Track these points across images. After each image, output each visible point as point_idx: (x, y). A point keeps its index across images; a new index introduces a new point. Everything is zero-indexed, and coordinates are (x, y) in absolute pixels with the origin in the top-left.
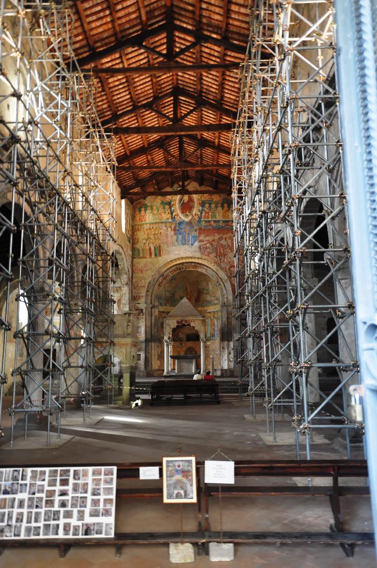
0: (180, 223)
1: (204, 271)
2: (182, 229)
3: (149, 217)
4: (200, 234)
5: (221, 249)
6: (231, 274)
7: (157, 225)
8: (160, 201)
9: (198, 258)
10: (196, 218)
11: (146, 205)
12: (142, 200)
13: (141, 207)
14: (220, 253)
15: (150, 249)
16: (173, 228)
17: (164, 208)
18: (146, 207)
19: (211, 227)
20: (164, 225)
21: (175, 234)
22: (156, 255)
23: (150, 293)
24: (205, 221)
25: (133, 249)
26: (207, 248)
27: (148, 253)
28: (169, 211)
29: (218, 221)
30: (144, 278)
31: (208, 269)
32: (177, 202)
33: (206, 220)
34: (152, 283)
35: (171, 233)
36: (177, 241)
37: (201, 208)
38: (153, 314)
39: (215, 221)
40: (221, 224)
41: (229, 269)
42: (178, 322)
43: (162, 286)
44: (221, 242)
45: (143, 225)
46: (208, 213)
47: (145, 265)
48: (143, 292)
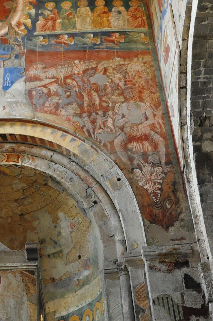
1: (41, 166)
4: (29, 62)
5: (95, 95)
6: (131, 159)
9: (23, 122)
10: (22, 31)
14: (92, 105)
19: (61, 49)
24: (44, 36)
26: (49, 94)
29: (83, 35)
31: (57, 157)
33: (48, 32)
37: (33, 11)
39: (72, 35)
40: (89, 40)
41: (124, 146)
44: (93, 80)
46: (54, 20)
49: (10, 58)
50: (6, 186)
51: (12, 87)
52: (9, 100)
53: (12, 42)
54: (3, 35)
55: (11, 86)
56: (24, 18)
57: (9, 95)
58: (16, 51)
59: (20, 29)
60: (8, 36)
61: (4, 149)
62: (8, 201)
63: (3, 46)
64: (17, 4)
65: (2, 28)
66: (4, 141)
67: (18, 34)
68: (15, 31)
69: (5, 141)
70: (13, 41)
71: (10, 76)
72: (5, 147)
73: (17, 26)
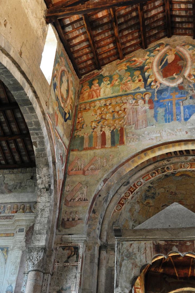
0: (160, 92)
2: (164, 99)
3: (105, 90)
7: (118, 100)
8: (125, 68)
11: (101, 75)
12: (96, 71)
13: (93, 80)
15: (104, 135)
16: (147, 98)
17: (132, 76)
18: (101, 78)
20: (130, 97)
21: (151, 108)
22: (113, 143)
23: (99, 217)
25: (72, 137)
27: (99, 141)
28: (141, 78)
30: (87, 184)
32: (155, 64)
34: (103, 195)
35: (143, 107)
36: (155, 116)
38: (104, 262)
42: (158, 249)
43: (127, 206)
45: (94, 101)
47: (93, 161)
48: (83, 212)
49: (186, 99)
50: (189, 184)
51: (190, 118)
52: (189, 127)
53: (186, 88)
54: (179, 84)
55: (190, 117)
56: (193, 71)
57: (189, 124)
58: (190, 94)
59: (191, 79)
60: (183, 84)
61: (188, 160)
62: (191, 194)
63: (180, 91)
64: (187, 62)
65: (178, 79)
66: (188, 155)
67: (190, 82)
68: (188, 81)
69: (189, 155)
70: (187, 87)
71: (188, 111)
72: (189, 158)
73: (188, 77)
